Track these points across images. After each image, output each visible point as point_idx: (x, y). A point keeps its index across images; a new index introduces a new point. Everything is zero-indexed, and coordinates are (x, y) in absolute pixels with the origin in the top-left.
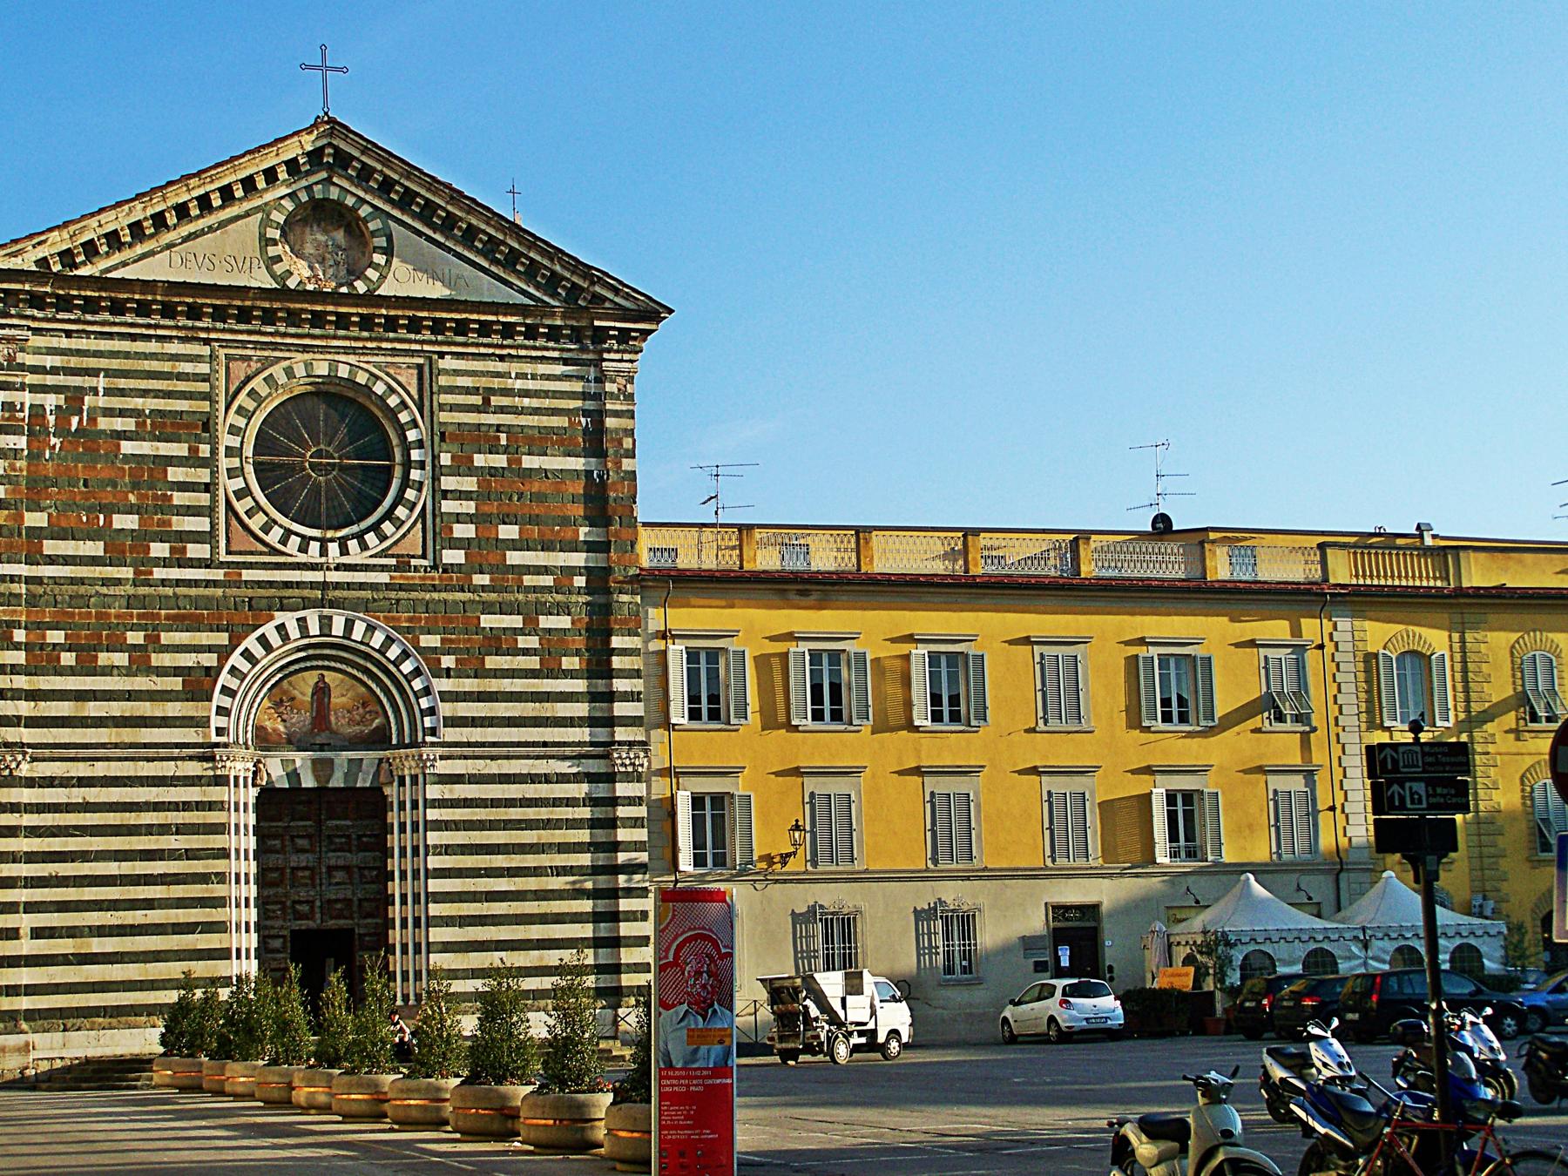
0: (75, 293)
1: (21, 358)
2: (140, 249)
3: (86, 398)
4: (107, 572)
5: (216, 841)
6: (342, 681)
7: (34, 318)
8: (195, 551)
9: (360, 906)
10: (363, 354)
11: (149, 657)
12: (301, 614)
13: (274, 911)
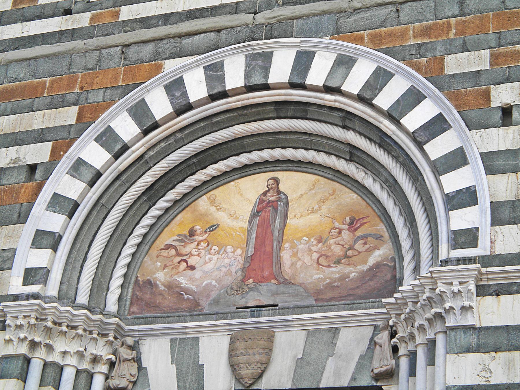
6: (314, 185)
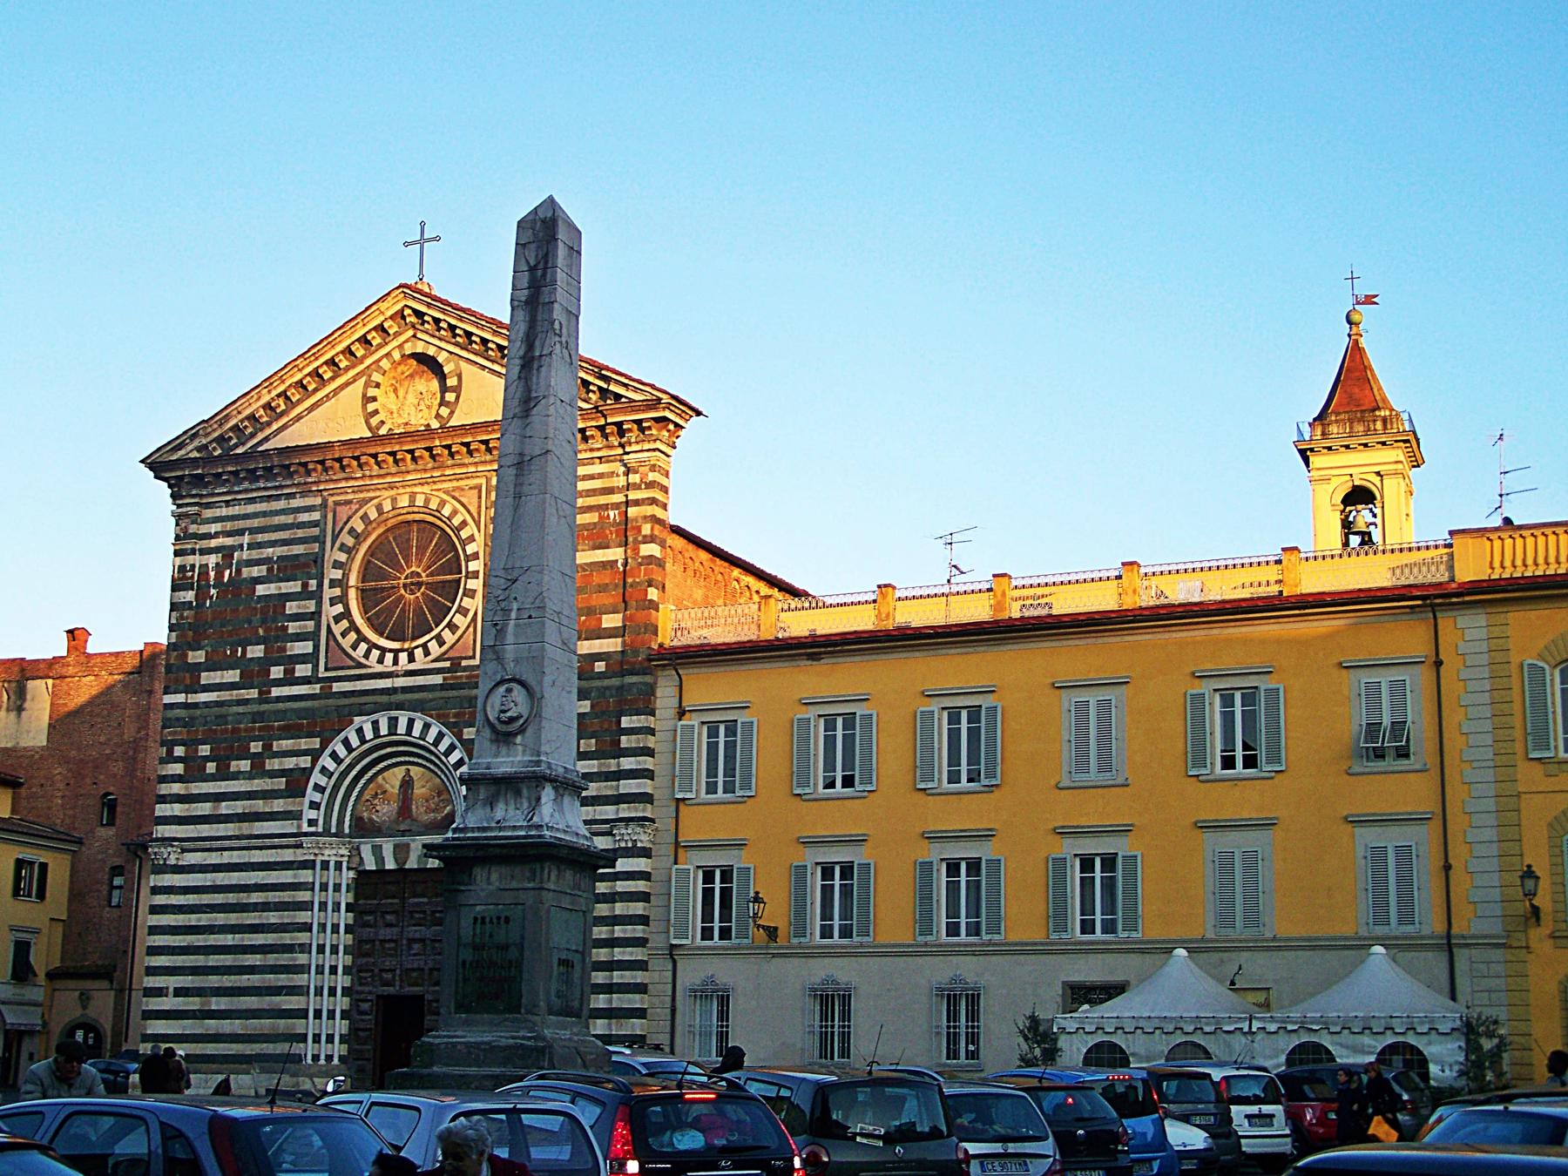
0: (220, 470)
1: (193, 528)
2: (275, 426)
3: (236, 554)
4: (241, 695)
5: (302, 917)
7: (201, 496)
8: (302, 670)
9: (430, 974)
10: (434, 482)
11: (264, 762)
12: (374, 717)
13: (365, 978)
